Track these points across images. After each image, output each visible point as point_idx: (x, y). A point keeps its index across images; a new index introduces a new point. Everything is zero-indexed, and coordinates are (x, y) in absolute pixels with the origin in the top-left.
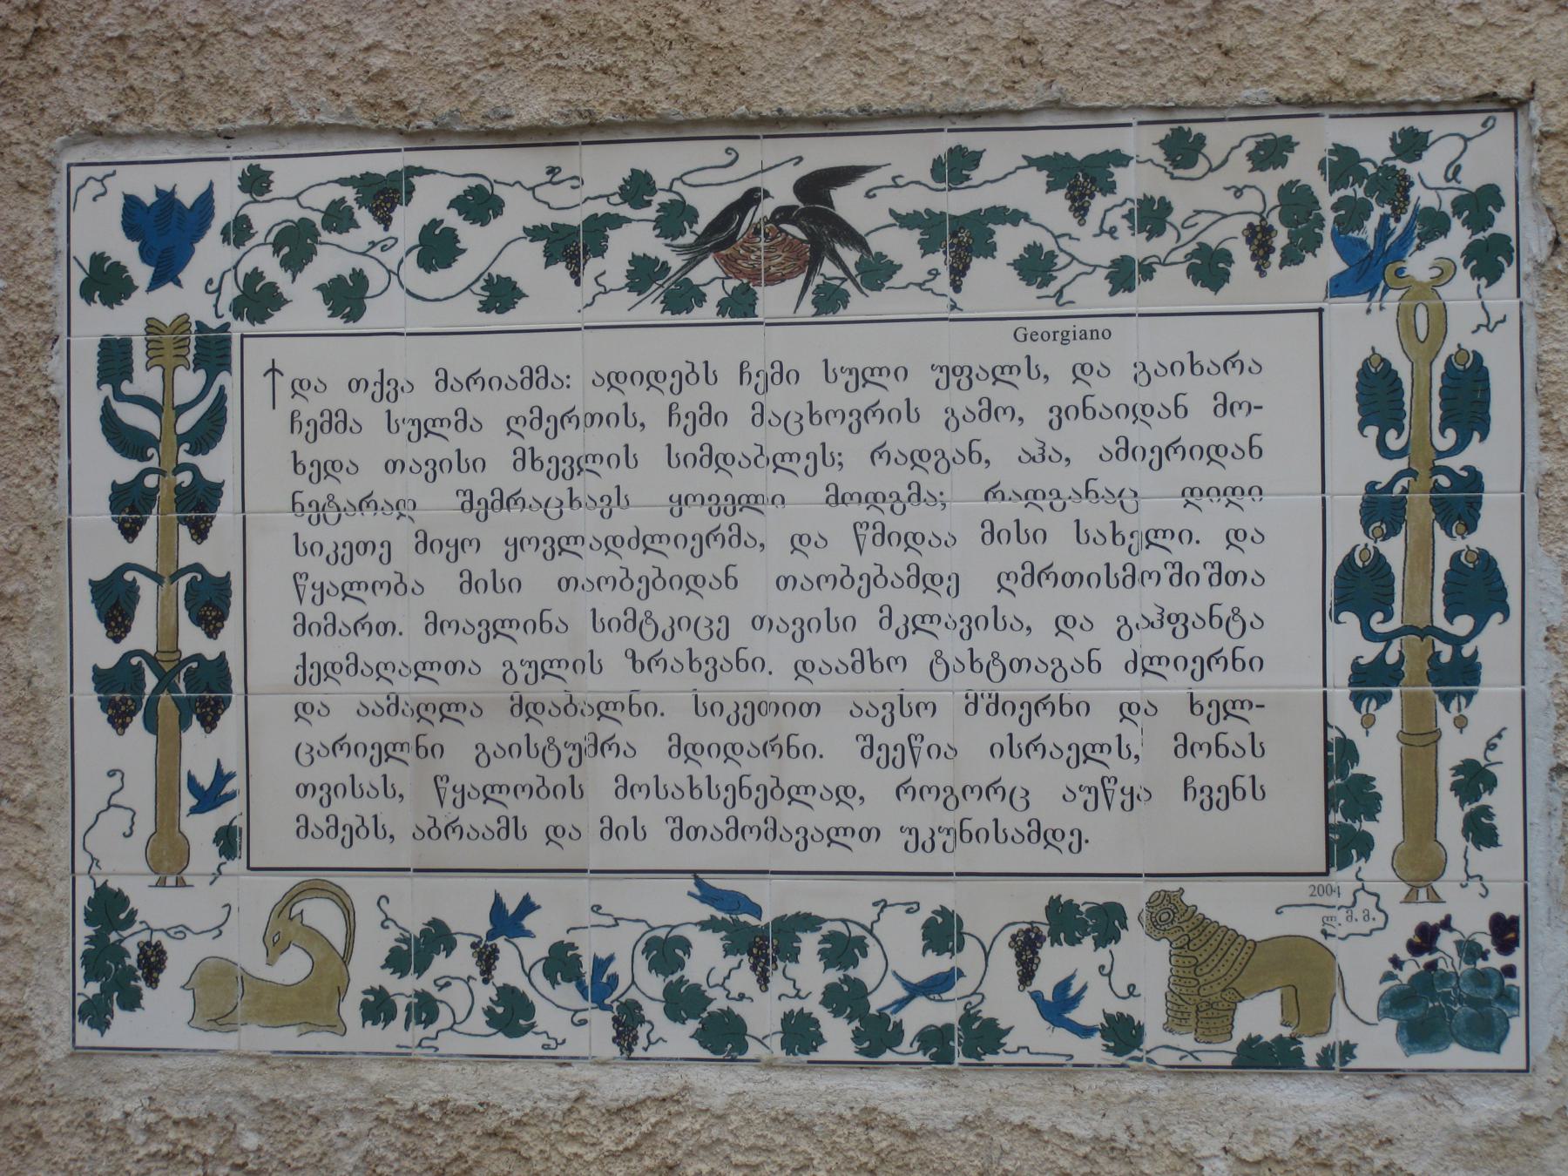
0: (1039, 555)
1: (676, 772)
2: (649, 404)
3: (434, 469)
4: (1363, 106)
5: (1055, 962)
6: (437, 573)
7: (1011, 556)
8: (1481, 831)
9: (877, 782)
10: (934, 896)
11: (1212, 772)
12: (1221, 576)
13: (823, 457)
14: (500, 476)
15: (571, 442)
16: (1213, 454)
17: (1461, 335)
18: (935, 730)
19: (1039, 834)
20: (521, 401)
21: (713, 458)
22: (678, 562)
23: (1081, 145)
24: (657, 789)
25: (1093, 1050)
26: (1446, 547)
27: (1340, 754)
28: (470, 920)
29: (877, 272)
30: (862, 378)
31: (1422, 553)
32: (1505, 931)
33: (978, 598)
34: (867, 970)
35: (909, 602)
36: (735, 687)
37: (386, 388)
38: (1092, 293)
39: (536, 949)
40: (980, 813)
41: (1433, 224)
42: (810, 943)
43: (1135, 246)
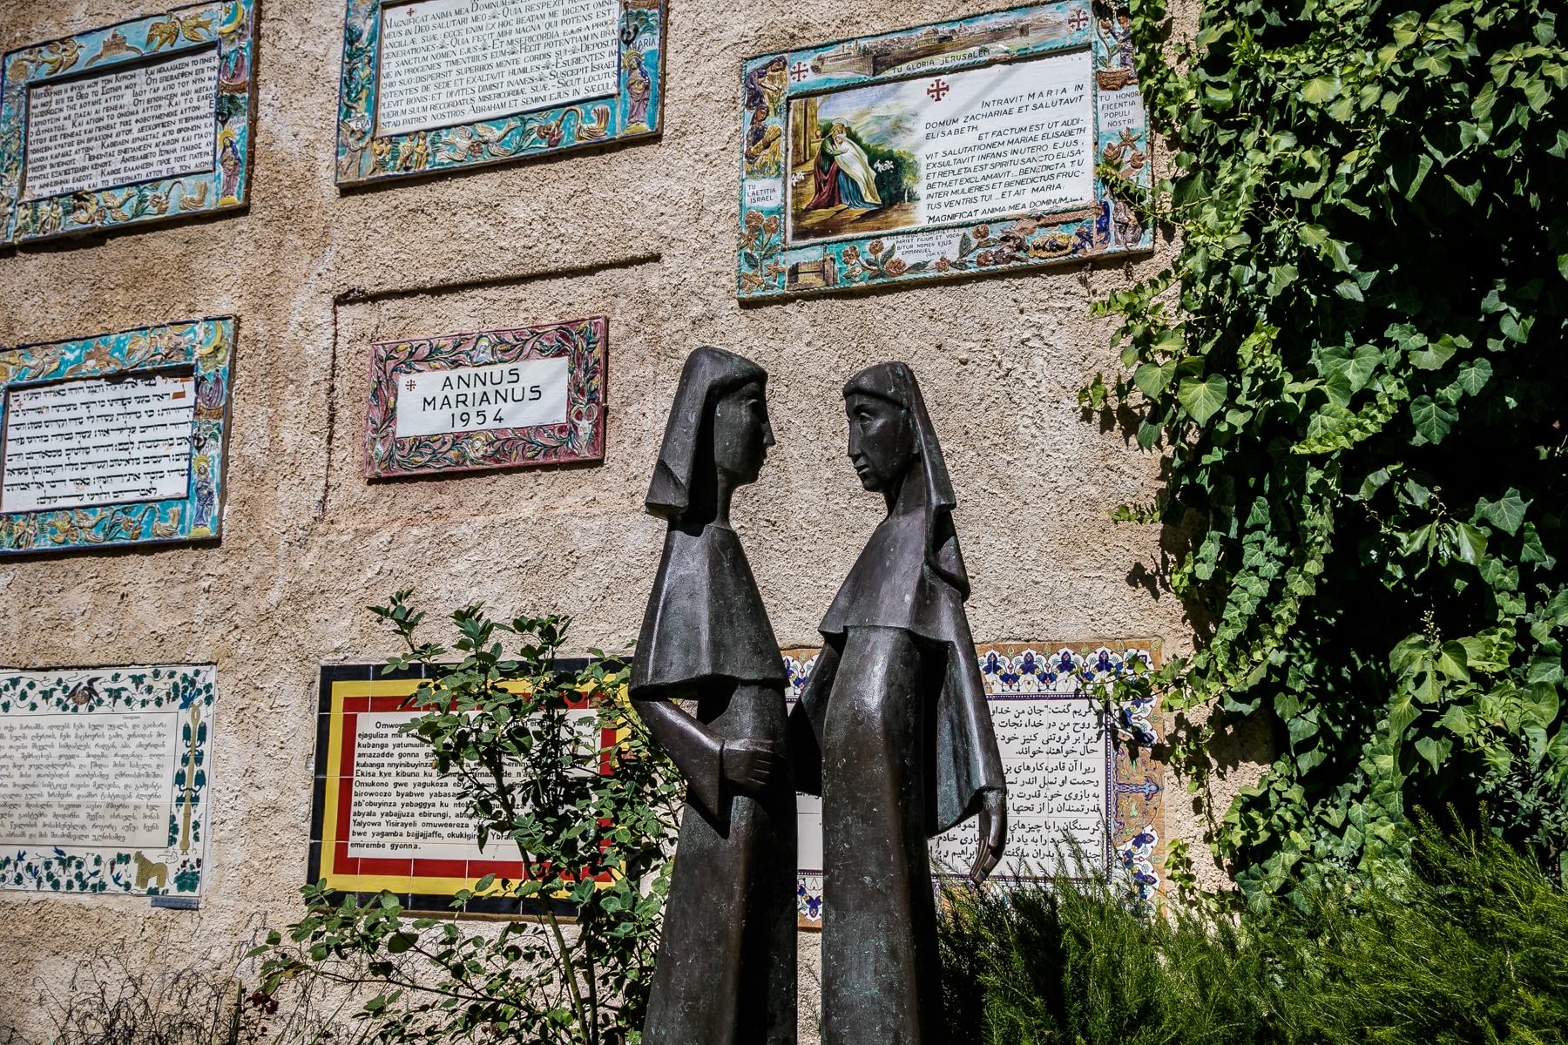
0: (122, 770)
1: (54, 821)
2: (57, 733)
3: (18, 747)
4: (188, 664)
5: (119, 868)
6: (15, 772)
7: (118, 770)
8: (196, 838)
9: (89, 824)
10: (98, 852)
11: (149, 822)
12: (156, 776)
13: (87, 746)
14: (29, 750)
15: (43, 742)
16: (156, 746)
17: (202, 719)
18: (101, 811)
19: (117, 837)
20: (34, 732)
21: (67, 746)
22: (59, 771)
23: (138, 672)
24: (50, 825)
25: (122, 890)
26: (196, 769)
27: (173, 818)
28: (14, 857)
29: (100, 702)
30: (95, 727)
31: (191, 770)
32: (199, 862)
33: (110, 781)
34: (83, 870)
35: (99, 781)
36: (68, 800)
37: (11, 729)
38: (137, 707)
39: (25, 864)
40: (107, 831)
41: (199, 692)
42: (74, 863)
43: (146, 697)
